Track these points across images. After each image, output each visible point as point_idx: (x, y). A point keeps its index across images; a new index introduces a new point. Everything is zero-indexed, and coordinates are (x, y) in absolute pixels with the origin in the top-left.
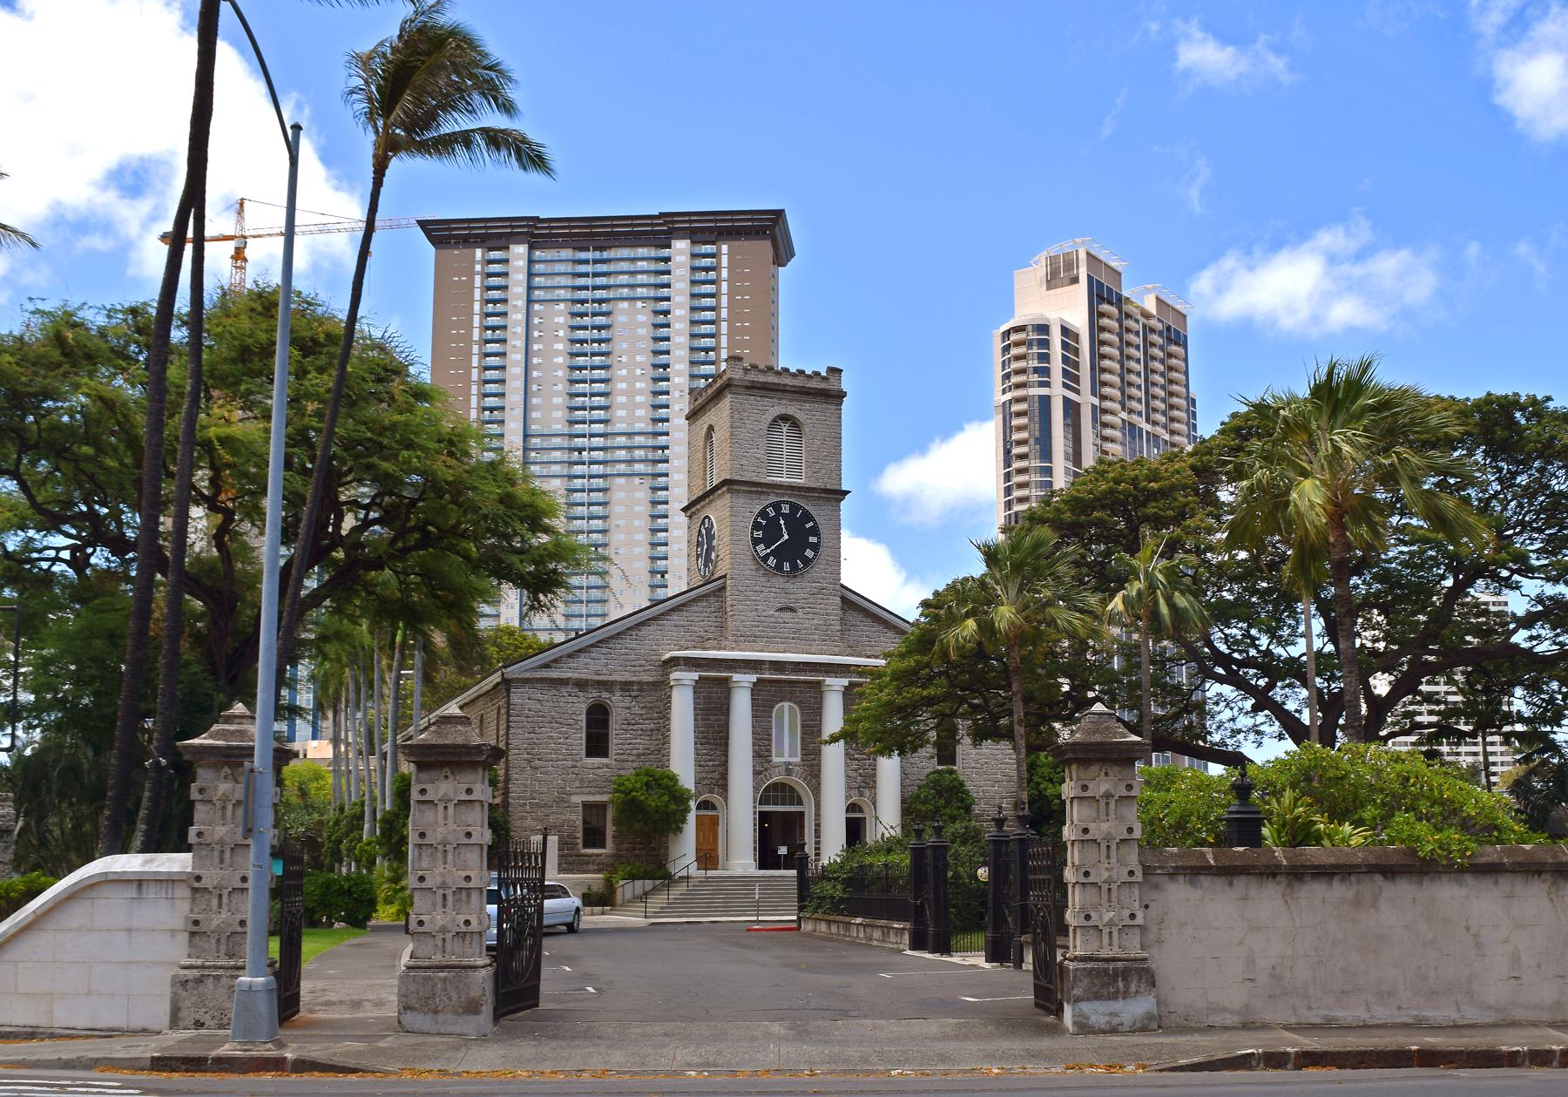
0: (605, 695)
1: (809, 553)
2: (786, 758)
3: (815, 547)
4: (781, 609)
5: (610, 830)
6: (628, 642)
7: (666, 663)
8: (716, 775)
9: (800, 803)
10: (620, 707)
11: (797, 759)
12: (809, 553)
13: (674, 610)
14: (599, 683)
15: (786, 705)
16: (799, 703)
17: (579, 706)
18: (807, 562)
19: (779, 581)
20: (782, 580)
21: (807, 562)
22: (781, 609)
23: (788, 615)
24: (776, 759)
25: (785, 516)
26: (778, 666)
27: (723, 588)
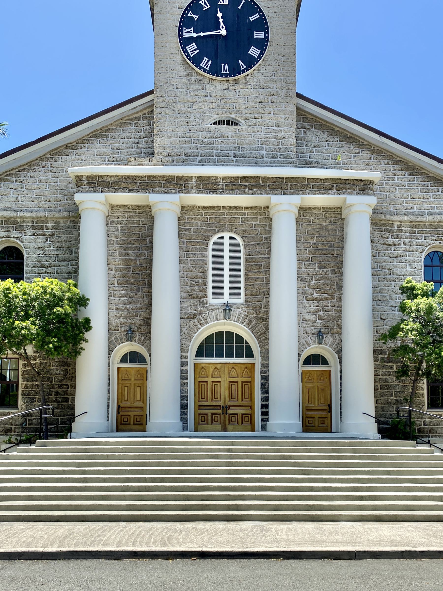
1: (254, 51)
3: (262, 45)
4: (216, 123)
8: (137, 321)
9: (250, 354)
11: (241, 301)
12: (254, 51)
13: (95, 135)
15: (226, 236)
16: (243, 234)
19: (217, 86)
20: (219, 87)
21: (251, 62)
22: (216, 123)
23: (224, 128)
24: (211, 301)
25: (223, 8)
26: (208, 185)
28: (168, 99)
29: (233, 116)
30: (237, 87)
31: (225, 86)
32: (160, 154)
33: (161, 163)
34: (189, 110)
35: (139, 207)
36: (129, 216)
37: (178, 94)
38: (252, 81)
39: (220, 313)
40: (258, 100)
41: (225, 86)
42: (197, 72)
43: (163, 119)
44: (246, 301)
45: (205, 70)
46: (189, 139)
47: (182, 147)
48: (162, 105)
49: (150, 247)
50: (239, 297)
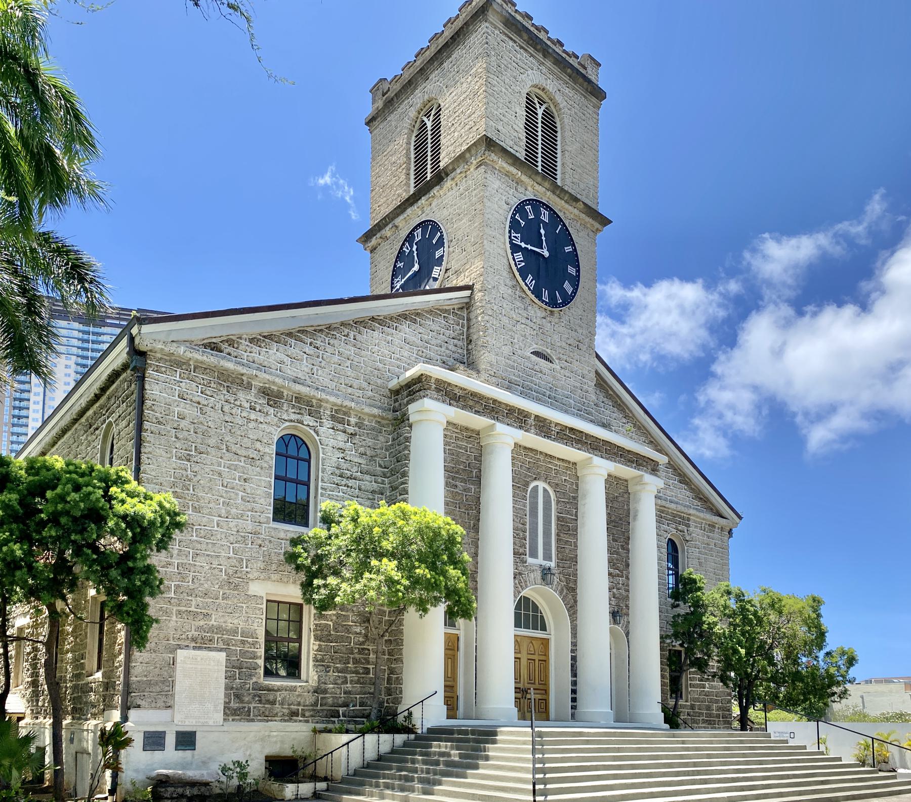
0: (308, 420)
1: (568, 287)
2: (540, 561)
4: (536, 353)
5: (309, 648)
6: (342, 345)
7: (396, 392)
9: (544, 628)
10: (330, 447)
12: (568, 287)
14: (299, 399)
17: (271, 428)
18: (563, 293)
19: (537, 311)
21: (567, 300)
22: (536, 353)
27: (468, 306)
28: (495, 308)
29: (549, 351)
30: (555, 320)
31: (544, 314)
32: (486, 370)
33: (487, 382)
34: (514, 329)
35: (467, 429)
36: (457, 438)
37: (505, 306)
38: (565, 319)
39: (538, 574)
40: (569, 342)
41: (544, 314)
42: (521, 288)
43: (490, 331)
44: (558, 566)
45: (529, 289)
46: (512, 363)
47: (507, 371)
48: (490, 312)
49: (478, 481)
50: (550, 559)
